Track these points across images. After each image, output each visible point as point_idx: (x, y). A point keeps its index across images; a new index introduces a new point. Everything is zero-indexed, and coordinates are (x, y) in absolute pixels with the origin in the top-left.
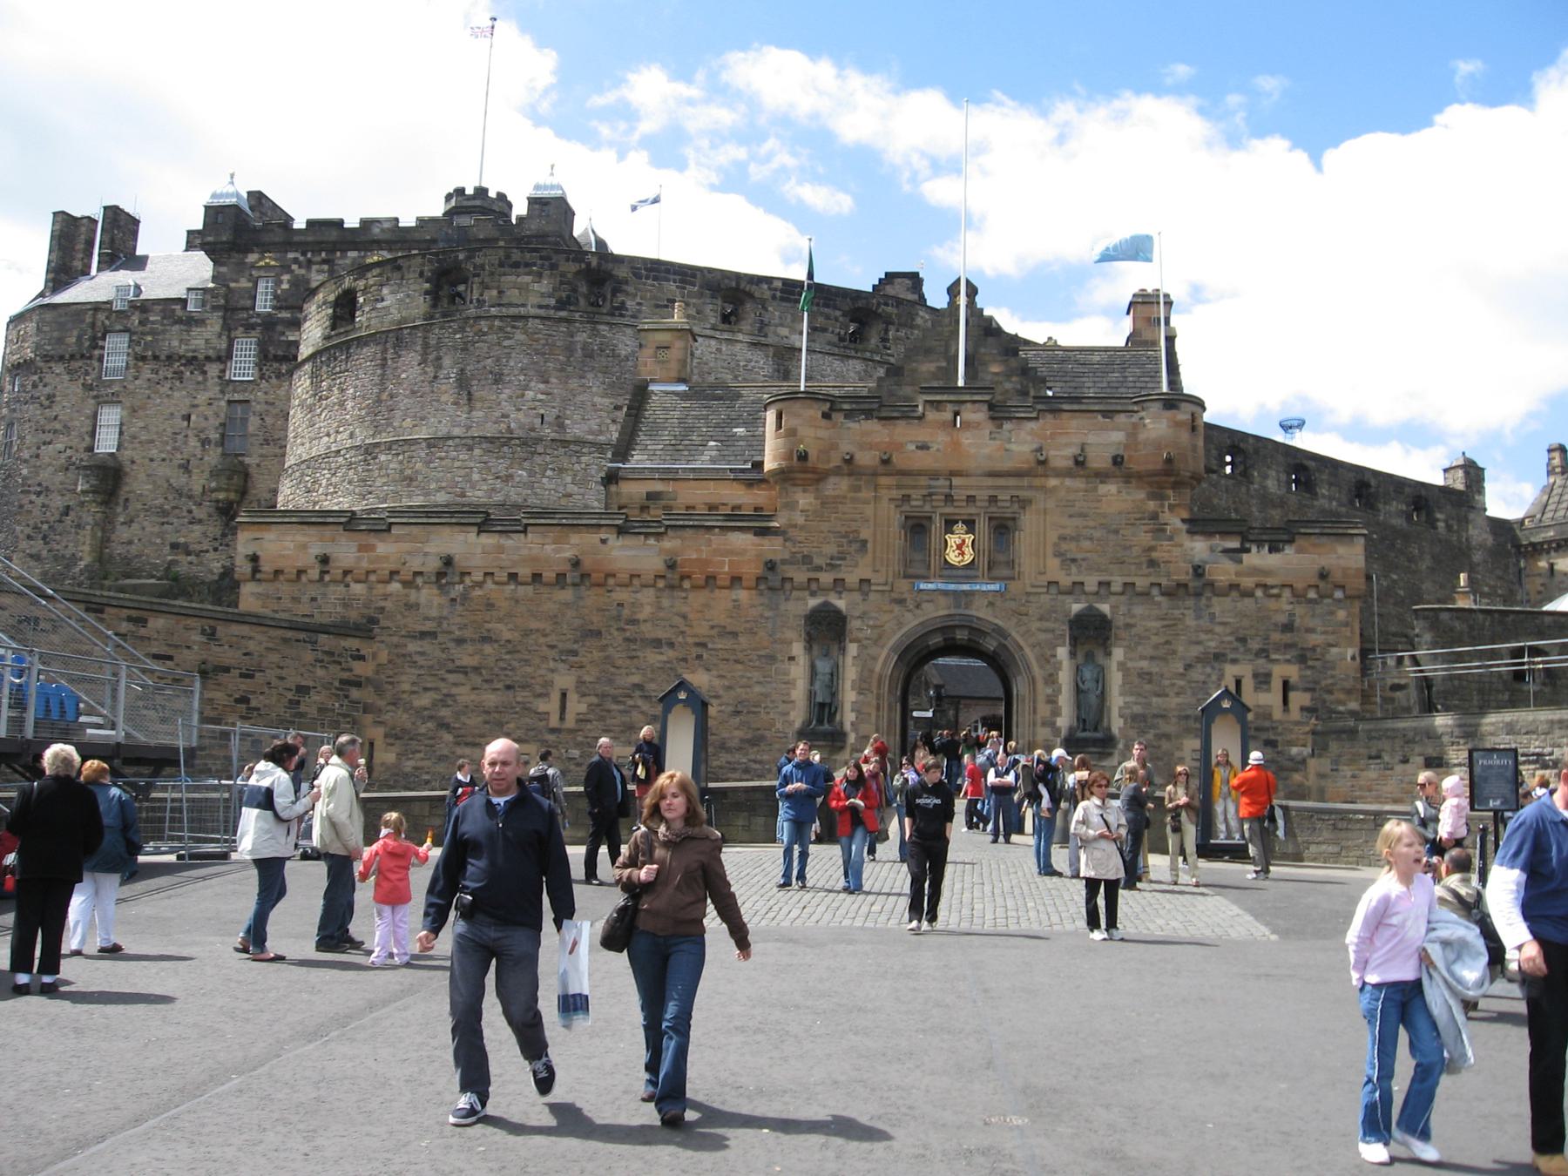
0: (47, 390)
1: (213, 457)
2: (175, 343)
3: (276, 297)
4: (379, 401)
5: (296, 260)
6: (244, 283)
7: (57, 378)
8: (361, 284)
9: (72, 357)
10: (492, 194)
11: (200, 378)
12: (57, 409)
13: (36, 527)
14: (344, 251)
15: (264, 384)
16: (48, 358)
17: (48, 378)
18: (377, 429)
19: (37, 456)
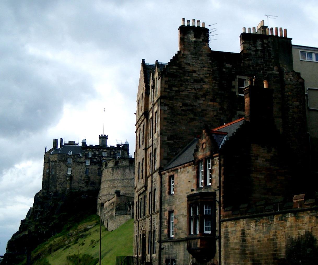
0: (60, 165)
1: (85, 175)
2: (79, 160)
3: (92, 155)
4: (124, 174)
5: (94, 150)
6: (87, 153)
7: (61, 163)
8: (120, 160)
9: (64, 161)
10: (106, 136)
11: (82, 165)
12: (61, 168)
13: (60, 183)
14: (101, 149)
15: (91, 166)
16: (60, 161)
17: (60, 163)
18: (124, 177)
19: (59, 174)
